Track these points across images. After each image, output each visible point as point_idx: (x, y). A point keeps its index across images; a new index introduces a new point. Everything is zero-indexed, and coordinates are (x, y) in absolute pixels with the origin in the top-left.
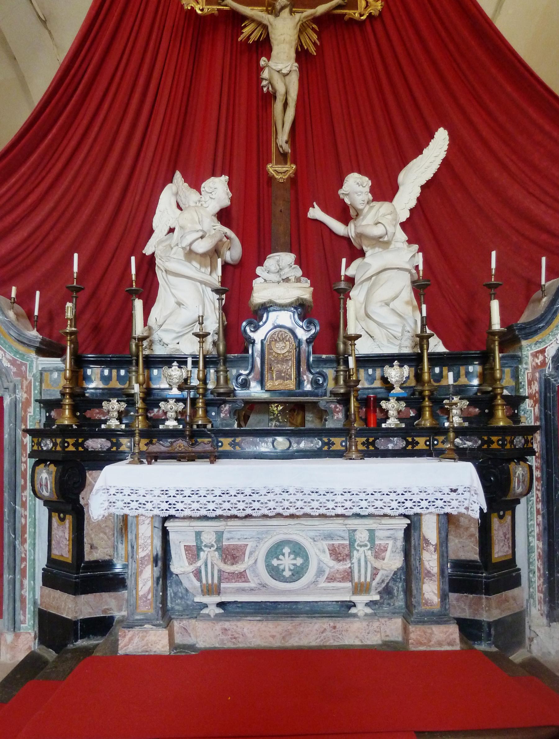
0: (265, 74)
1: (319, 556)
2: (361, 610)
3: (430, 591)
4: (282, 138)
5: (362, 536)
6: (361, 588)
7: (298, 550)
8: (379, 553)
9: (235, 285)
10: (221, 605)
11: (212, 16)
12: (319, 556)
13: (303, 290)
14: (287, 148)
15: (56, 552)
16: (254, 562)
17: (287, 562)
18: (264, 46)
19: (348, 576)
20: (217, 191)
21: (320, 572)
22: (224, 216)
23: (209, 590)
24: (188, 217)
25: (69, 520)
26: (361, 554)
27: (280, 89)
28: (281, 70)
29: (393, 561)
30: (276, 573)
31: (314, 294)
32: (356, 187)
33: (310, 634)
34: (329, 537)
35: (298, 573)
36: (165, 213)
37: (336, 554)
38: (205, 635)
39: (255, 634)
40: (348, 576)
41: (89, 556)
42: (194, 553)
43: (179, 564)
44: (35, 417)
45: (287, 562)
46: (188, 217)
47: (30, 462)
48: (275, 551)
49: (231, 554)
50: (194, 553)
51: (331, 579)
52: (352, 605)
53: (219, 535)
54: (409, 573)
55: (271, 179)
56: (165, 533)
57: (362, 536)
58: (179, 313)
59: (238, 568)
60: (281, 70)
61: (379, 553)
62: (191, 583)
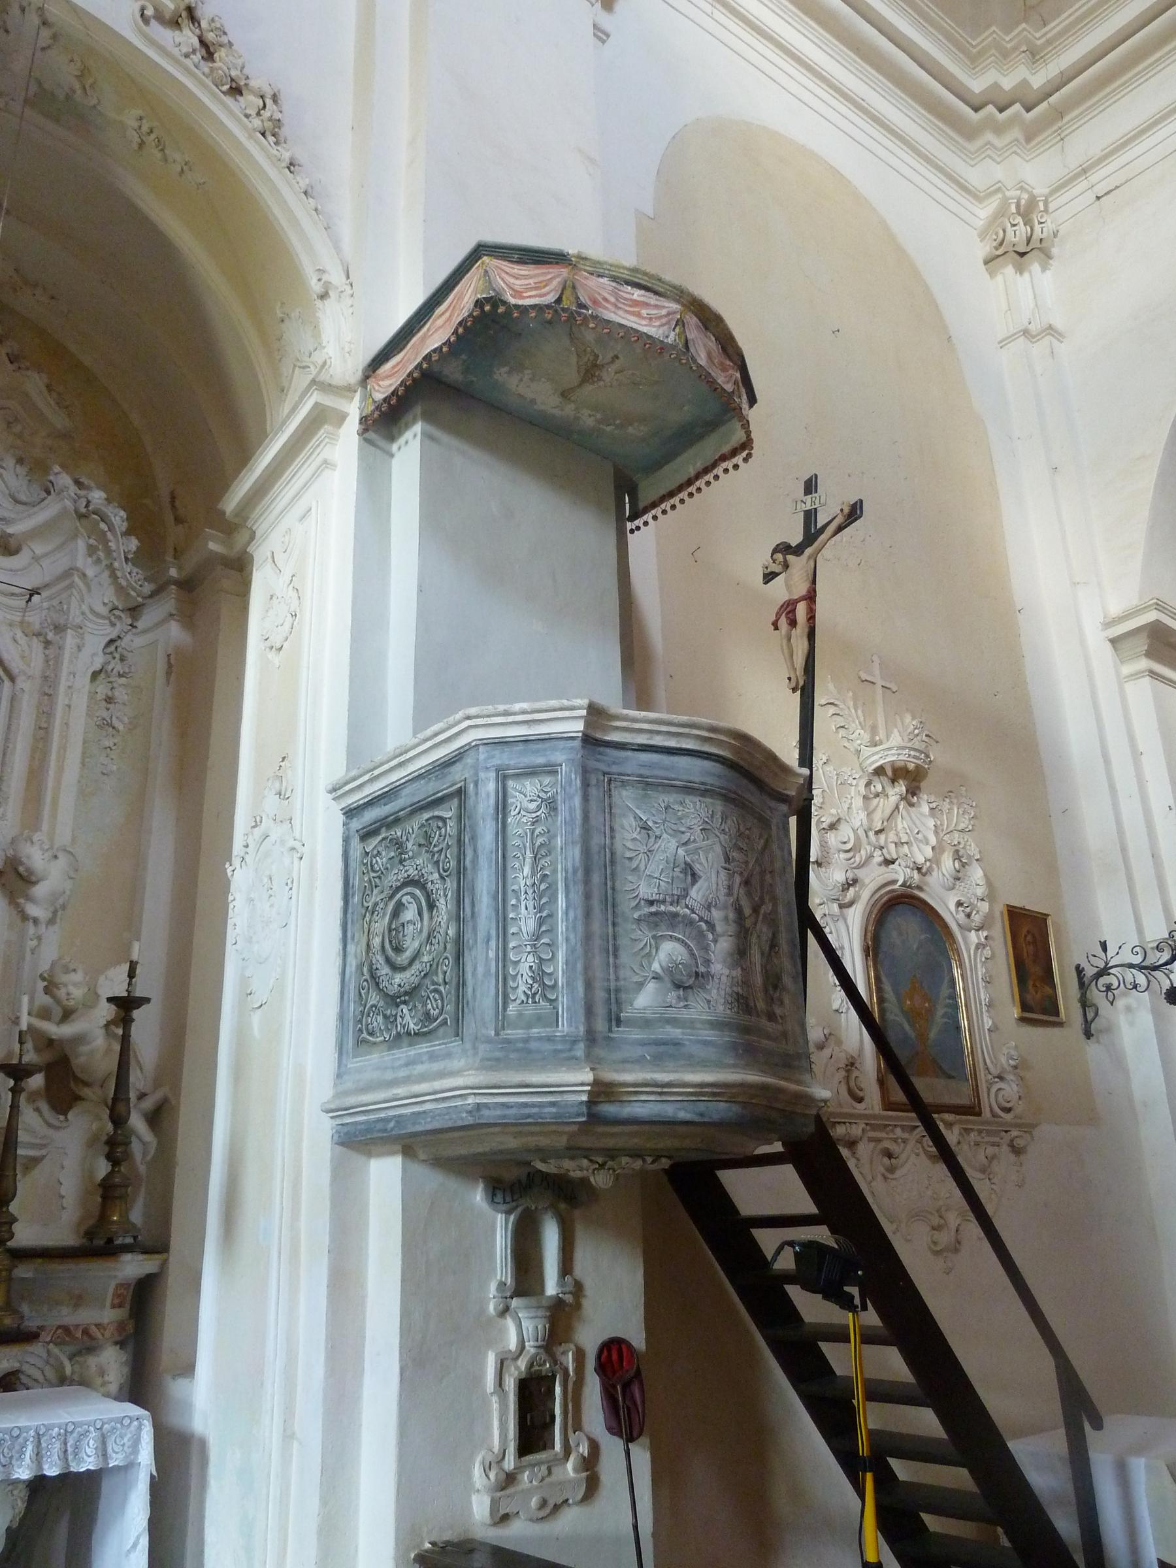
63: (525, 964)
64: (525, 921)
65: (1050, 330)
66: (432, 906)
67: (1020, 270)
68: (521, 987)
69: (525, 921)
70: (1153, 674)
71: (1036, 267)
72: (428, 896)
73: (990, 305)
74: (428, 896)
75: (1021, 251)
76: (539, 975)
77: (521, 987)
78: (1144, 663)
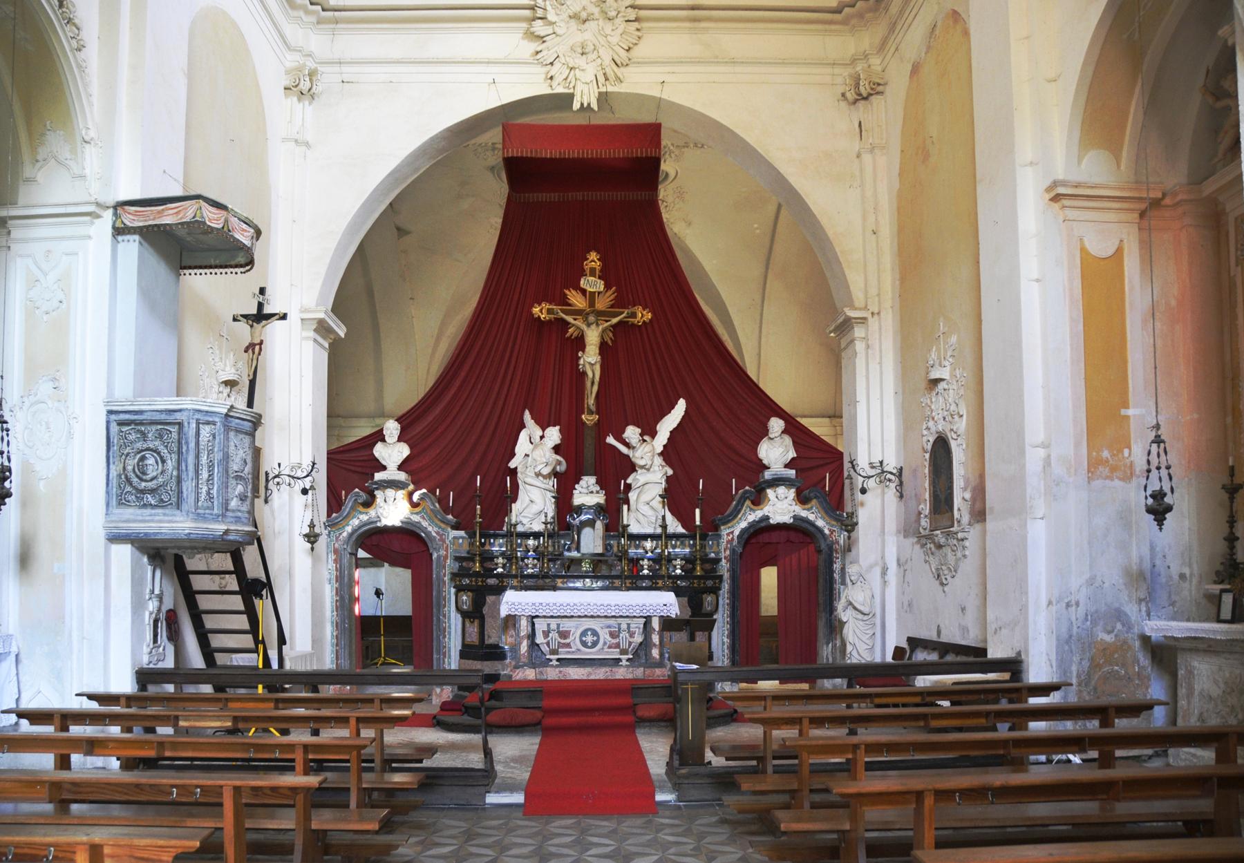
0: (581, 362)
1: (604, 635)
2: (624, 663)
3: (655, 653)
4: (591, 401)
5: (624, 626)
6: (624, 652)
7: (595, 633)
8: (632, 635)
9: (564, 484)
10: (558, 660)
11: (550, 321)
12: (604, 635)
13: (600, 498)
14: (593, 408)
15: (468, 640)
16: (575, 639)
17: (589, 639)
18: (580, 342)
19: (617, 645)
20: (554, 435)
21: (605, 643)
22: (557, 449)
23: (554, 652)
24: (535, 450)
25: (476, 622)
26: (624, 635)
27: (590, 374)
28: (590, 359)
29: (638, 639)
30: (584, 644)
31: (606, 500)
32: (632, 433)
33: (600, 674)
34: (609, 627)
35: (595, 644)
36: (523, 445)
37: (612, 635)
38: (552, 674)
39: (575, 673)
40: (617, 645)
41: (488, 641)
42: (546, 634)
43: (540, 639)
44: (450, 566)
45: (589, 639)
46: (535, 450)
47: (453, 590)
48: (584, 634)
49: (564, 635)
50: (546, 634)
51: (610, 647)
52: (620, 660)
53: (558, 625)
54: (646, 645)
55: (584, 423)
56: (533, 624)
57: (624, 626)
58: (532, 507)
59: (567, 641)
60: (590, 359)
61: (632, 635)
62: (545, 648)
63: (205, 489)
64: (205, 475)
65: (307, 144)
66: (163, 462)
67: (299, 100)
68: (203, 496)
69: (205, 475)
70: (315, 340)
71: (307, 103)
72: (161, 458)
73: (284, 114)
74: (161, 458)
75: (302, 88)
76: (208, 493)
77: (203, 496)
78: (312, 334)
